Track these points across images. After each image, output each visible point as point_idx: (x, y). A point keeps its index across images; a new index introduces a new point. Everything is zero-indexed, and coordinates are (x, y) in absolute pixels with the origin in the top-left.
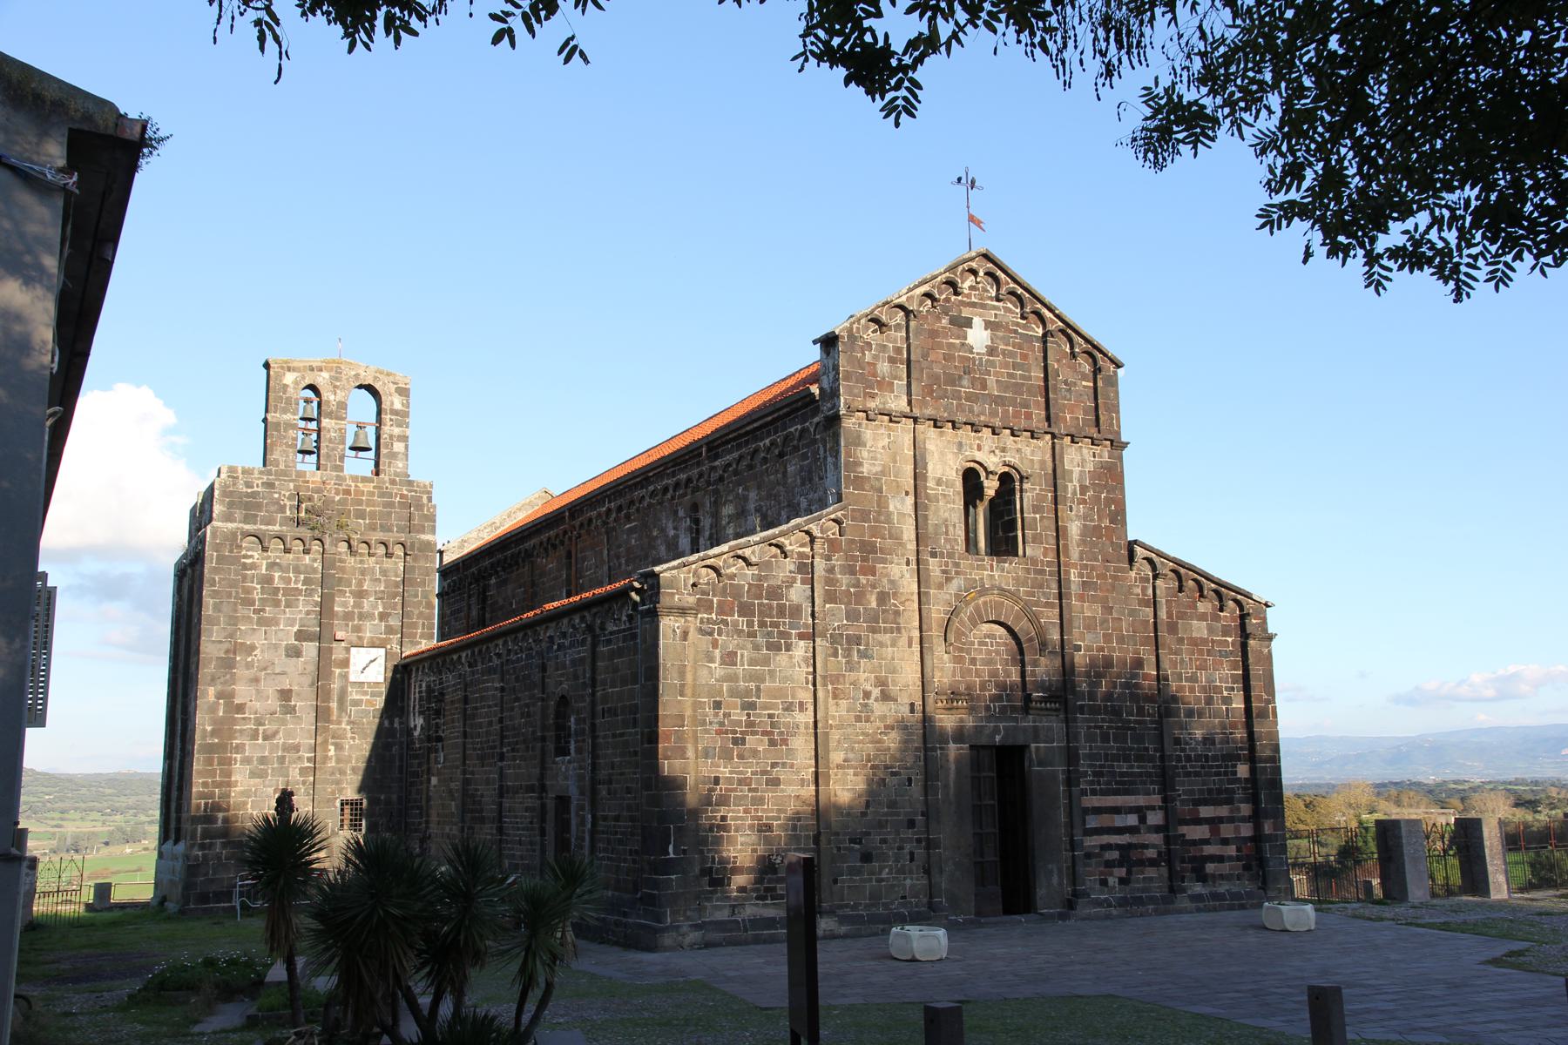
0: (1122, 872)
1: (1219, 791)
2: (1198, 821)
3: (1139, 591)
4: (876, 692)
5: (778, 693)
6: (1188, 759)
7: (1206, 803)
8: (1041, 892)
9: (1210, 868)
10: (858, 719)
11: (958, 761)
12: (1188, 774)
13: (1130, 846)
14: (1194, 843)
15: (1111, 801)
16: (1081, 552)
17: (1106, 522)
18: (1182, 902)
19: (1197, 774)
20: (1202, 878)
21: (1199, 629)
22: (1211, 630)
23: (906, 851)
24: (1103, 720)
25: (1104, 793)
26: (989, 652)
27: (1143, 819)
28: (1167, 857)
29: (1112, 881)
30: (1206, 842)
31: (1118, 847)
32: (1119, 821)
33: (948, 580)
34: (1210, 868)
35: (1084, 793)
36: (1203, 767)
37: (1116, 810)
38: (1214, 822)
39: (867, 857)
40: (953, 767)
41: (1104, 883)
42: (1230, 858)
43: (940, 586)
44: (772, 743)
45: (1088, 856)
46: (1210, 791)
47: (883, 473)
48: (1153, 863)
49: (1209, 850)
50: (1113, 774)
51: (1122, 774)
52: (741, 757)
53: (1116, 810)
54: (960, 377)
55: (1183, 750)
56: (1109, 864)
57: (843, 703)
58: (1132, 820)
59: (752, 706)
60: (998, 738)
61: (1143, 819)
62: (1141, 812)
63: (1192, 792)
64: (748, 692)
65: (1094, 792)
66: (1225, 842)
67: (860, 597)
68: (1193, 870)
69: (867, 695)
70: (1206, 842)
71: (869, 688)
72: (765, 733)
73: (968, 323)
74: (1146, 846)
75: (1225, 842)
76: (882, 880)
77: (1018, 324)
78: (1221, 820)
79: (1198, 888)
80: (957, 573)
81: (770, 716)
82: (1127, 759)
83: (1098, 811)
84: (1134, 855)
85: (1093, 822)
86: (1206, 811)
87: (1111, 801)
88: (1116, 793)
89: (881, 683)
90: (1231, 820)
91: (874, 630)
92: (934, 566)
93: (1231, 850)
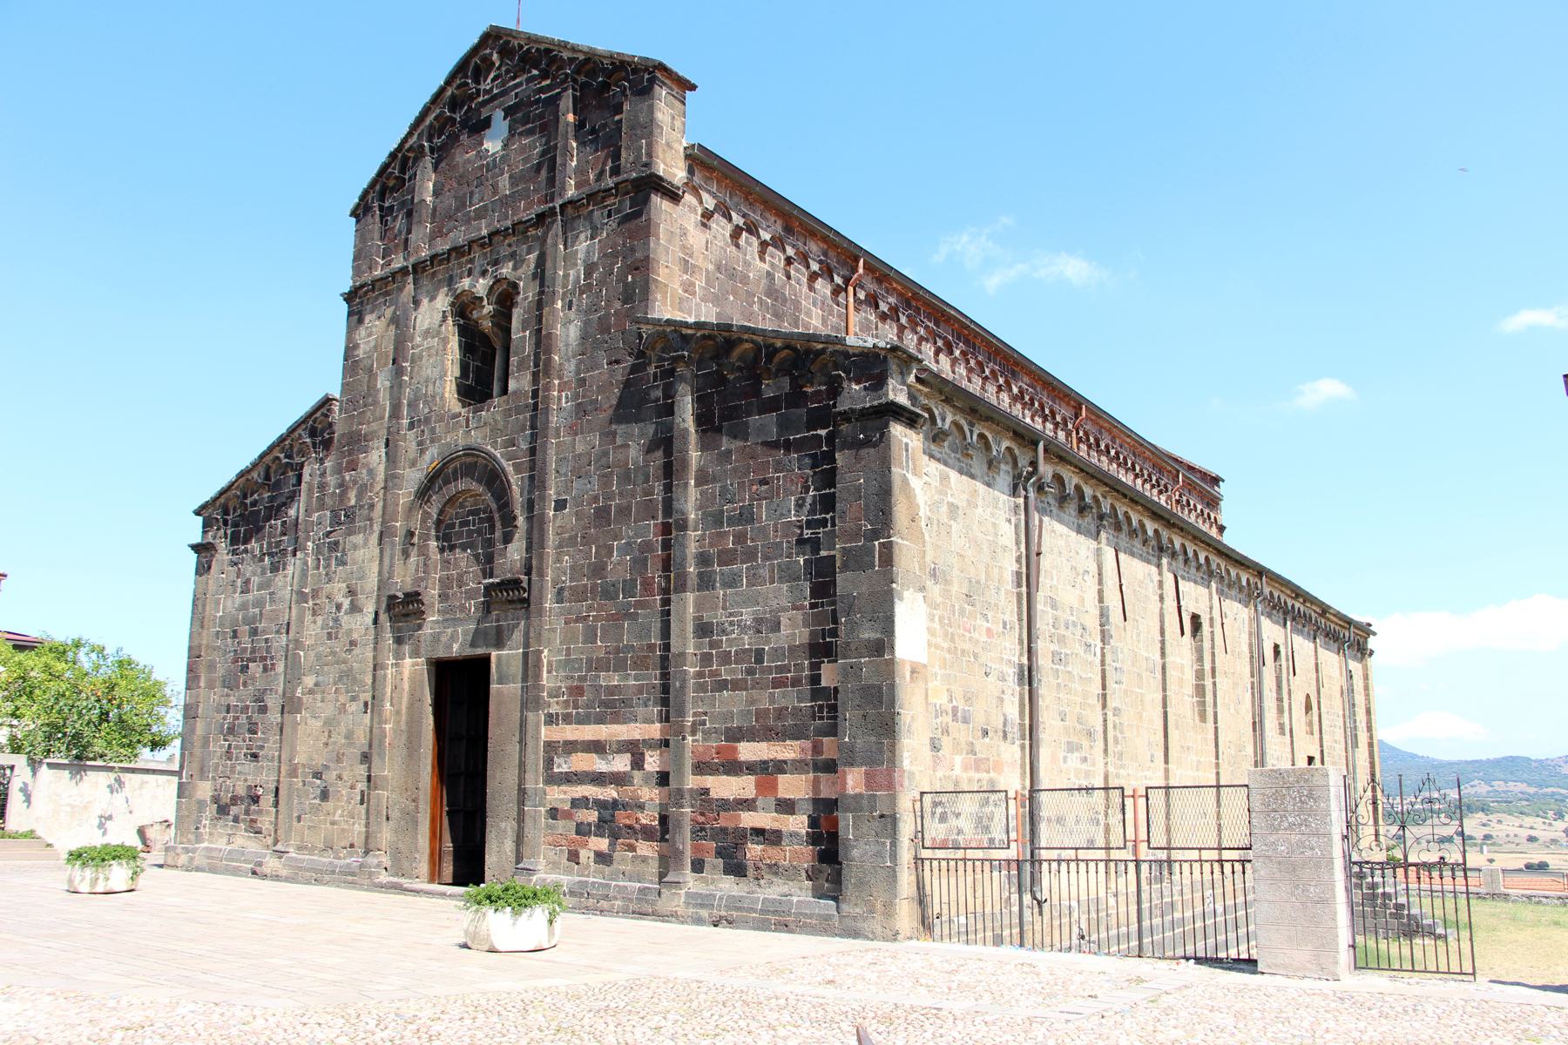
0: (603, 844)
1: (780, 713)
2: (733, 767)
3: (659, 393)
4: (346, 603)
5: (275, 616)
6: (725, 658)
7: (752, 735)
8: (491, 860)
9: (754, 850)
10: (329, 636)
11: (412, 679)
12: (722, 685)
13: (615, 804)
14: (725, 805)
15: (589, 732)
16: (577, 366)
17: (618, 305)
18: (675, 901)
19: (736, 685)
20: (736, 868)
21: (761, 429)
22: (784, 426)
23: (358, 791)
24: (590, 608)
25: (581, 721)
26: (470, 533)
27: (638, 763)
28: (664, 829)
29: (583, 854)
30: (747, 804)
31: (601, 805)
32: (600, 765)
33: (422, 452)
34: (754, 850)
35: (551, 720)
36: (750, 672)
37: (597, 747)
38: (767, 771)
39: (324, 795)
40: (406, 686)
41: (574, 857)
42: (793, 835)
43: (413, 464)
44: (265, 669)
45: (554, 813)
46: (761, 714)
47: (375, 347)
48: (647, 833)
49: (748, 820)
50: (597, 688)
51: (611, 690)
52: (245, 684)
53: (597, 747)
54: (472, 194)
55: (712, 645)
56: (582, 830)
57: (319, 620)
58: (621, 763)
59: (254, 632)
60: (455, 647)
61: (638, 763)
62: (635, 750)
63: (729, 716)
64: (254, 620)
65: (567, 719)
66: (787, 807)
67: (343, 495)
68: (719, 853)
69: (339, 607)
70: (747, 804)
71: (340, 599)
72: (263, 659)
73: (486, 123)
74: (641, 807)
75: (787, 807)
76: (333, 823)
77: (541, 90)
78: (780, 767)
79: (728, 886)
80: (432, 441)
81: (267, 640)
82: (620, 666)
83: (571, 747)
84: (622, 818)
85: (562, 766)
86: (748, 751)
87: (589, 732)
88: (600, 720)
89: (351, 592)
90: (798, 766)
91: (350, 533)
92: (409, 442)
93: (798, 823)
